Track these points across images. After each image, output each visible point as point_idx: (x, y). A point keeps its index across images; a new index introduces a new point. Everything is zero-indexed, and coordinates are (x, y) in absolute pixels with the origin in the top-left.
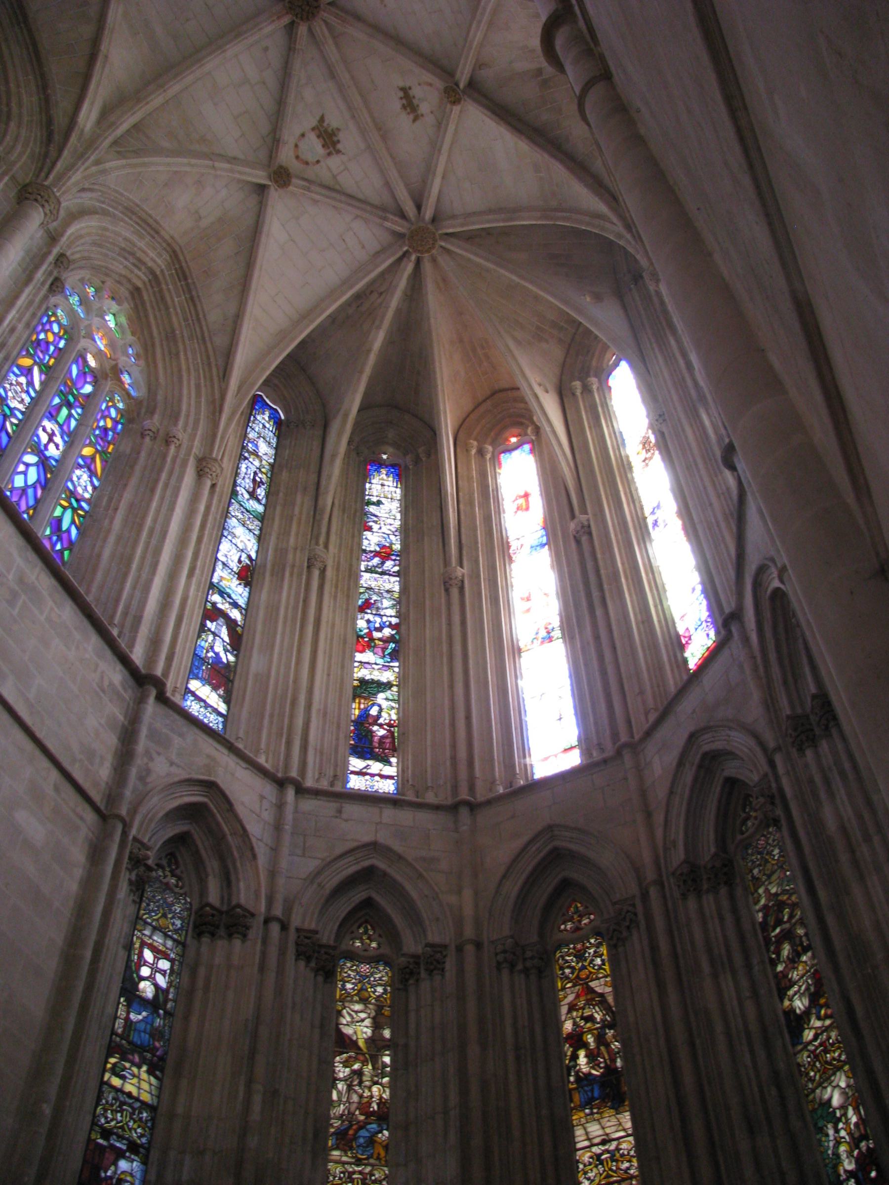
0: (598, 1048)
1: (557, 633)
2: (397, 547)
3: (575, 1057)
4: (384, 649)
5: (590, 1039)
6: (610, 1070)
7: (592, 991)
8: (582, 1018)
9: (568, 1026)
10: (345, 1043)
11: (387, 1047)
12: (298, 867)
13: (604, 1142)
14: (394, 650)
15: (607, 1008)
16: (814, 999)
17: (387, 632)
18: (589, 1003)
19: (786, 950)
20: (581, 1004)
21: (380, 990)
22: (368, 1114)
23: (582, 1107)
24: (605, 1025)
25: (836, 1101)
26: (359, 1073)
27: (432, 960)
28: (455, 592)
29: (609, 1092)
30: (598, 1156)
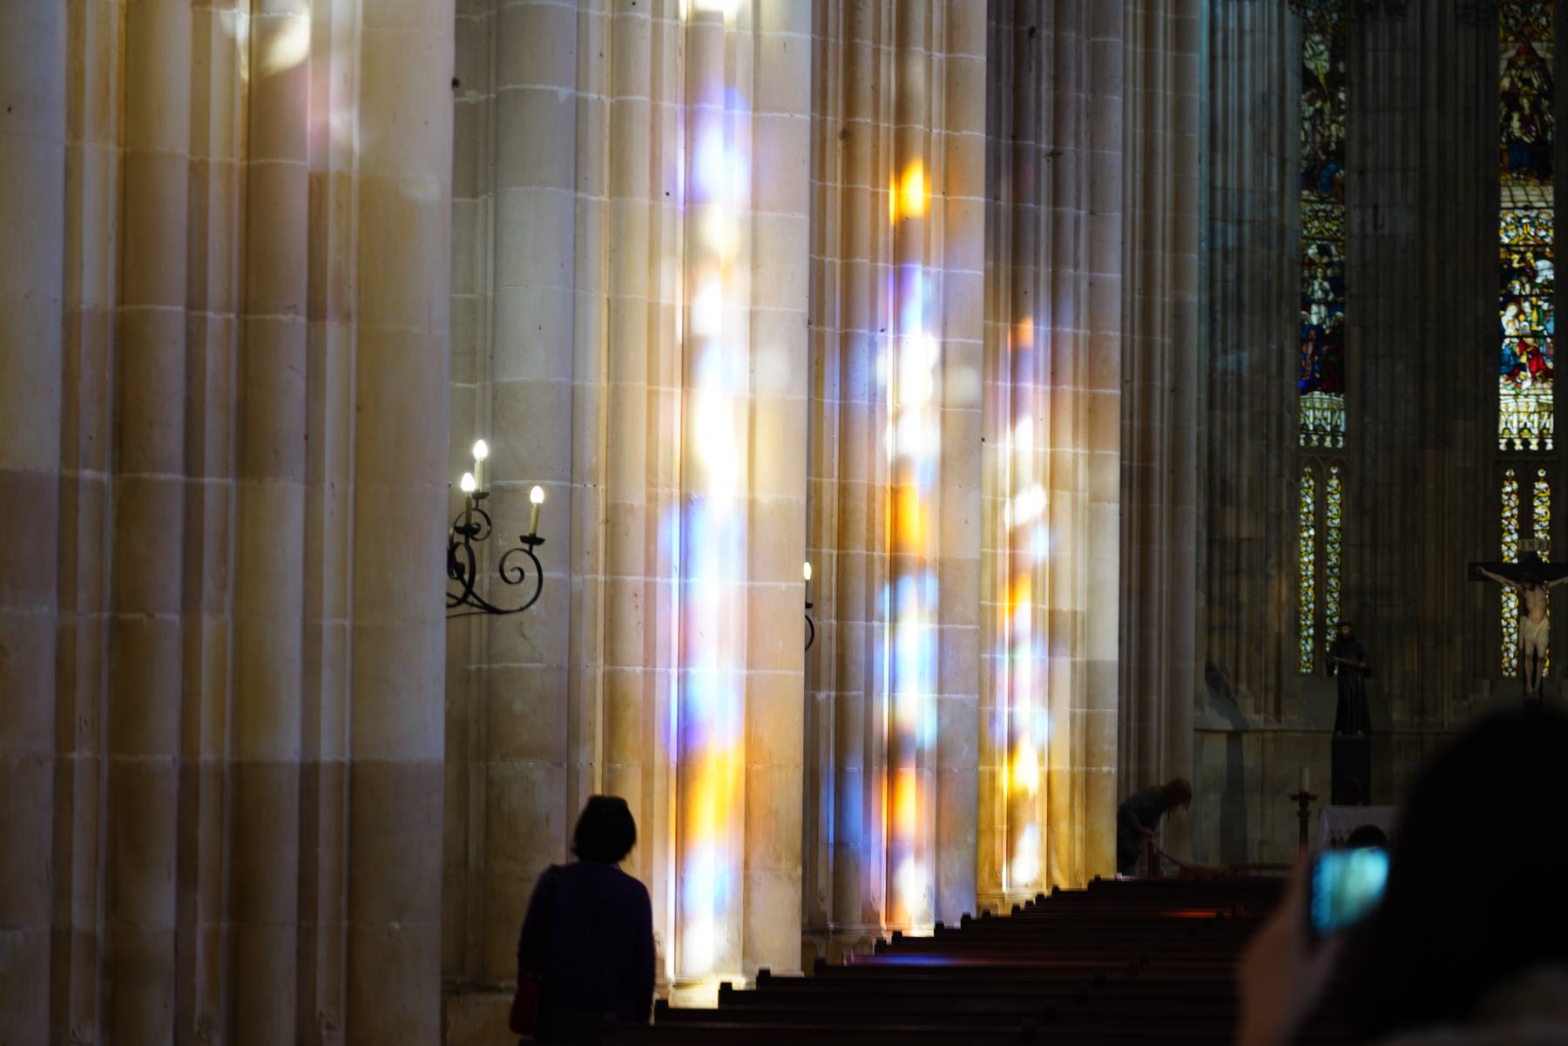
0: (1532, 115)
3: (1509, 118)
5: (1525, 103)
6: (1540, 140)
7: (1533, 51)
8: (1521, 78)
9: (1506, 83)
10: (1308, 79)
11: (1342, 83)
13: (1526, 208)
15: (1546, 77)
18: (1529, 64)
20: (1521, 63)
21: (1335, 16)
22: (1326, 152)
23: (1510, 170)
24: (1542, 94)
26: (1320, 112)
29: (1535, 162)
30: (1520, 219)
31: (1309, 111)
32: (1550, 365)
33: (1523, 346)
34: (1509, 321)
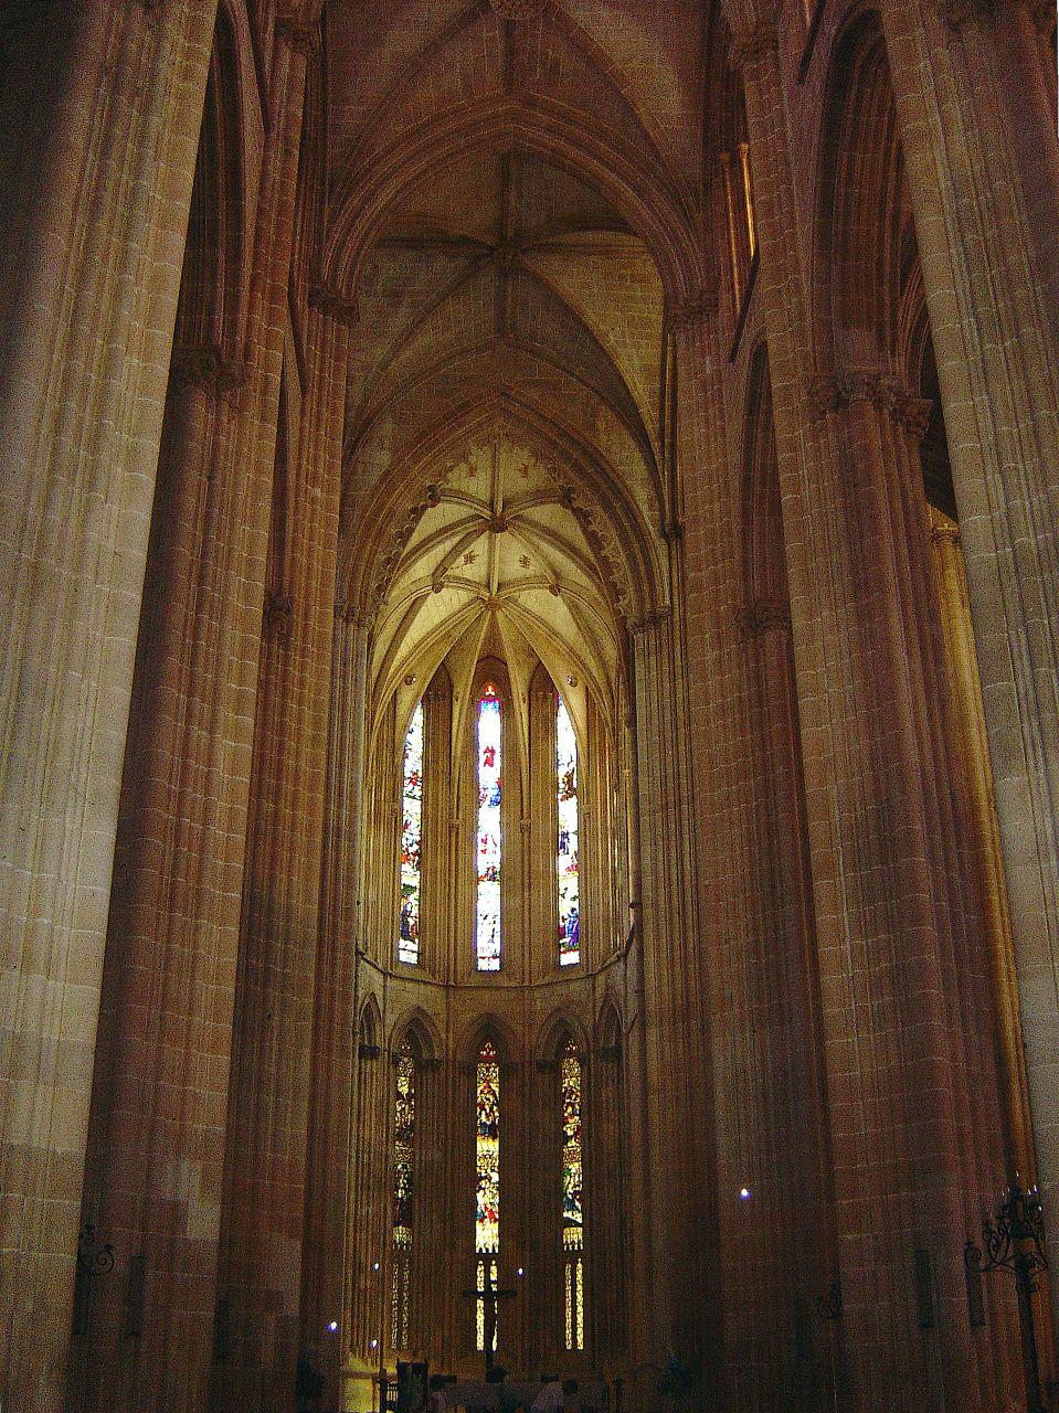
1: (498, 877)
2: (420, 774)
3: (480, 1114)
4: (414, 861)
5: (487, 1108)
10: (399, 1095)
12: (390, 1019)
14: (419, 863)
16: (576, 1134)
17: (416, 847)
19: (570, 1110)
25: (573, 1171)
26: (404, 1109)
27: (433, 1065)
28: (454, 834)
29: (492, 1132)
31: (399, 1109)
32: (497, 1216)
33: (486, 1208)
34: (479, 1195)
